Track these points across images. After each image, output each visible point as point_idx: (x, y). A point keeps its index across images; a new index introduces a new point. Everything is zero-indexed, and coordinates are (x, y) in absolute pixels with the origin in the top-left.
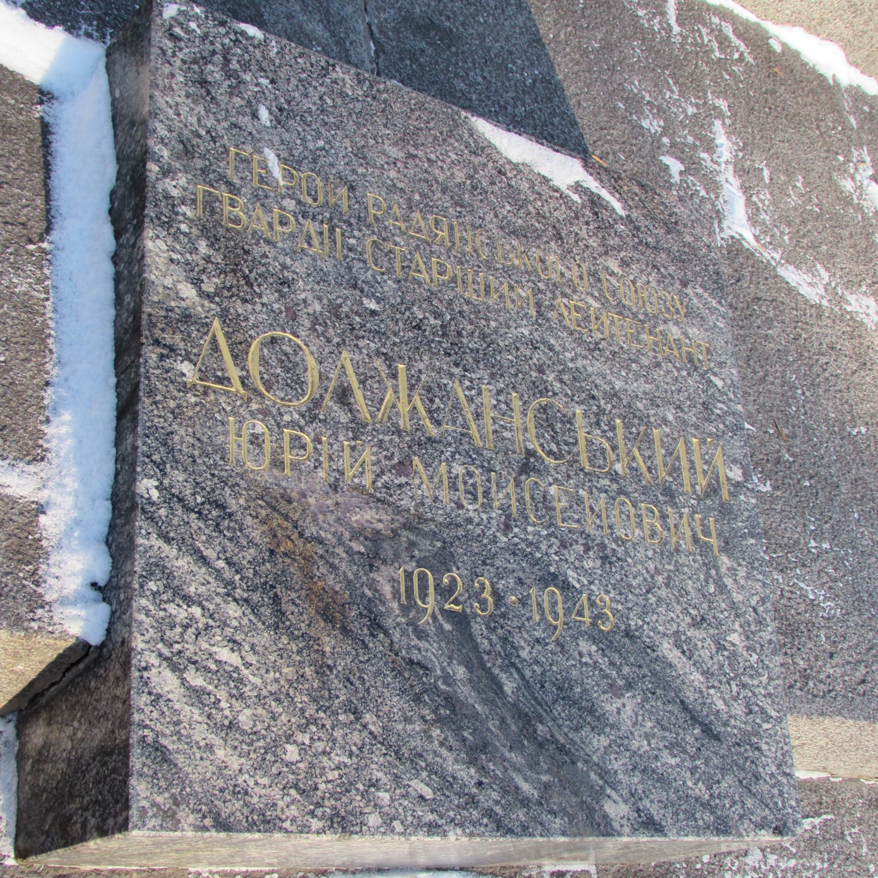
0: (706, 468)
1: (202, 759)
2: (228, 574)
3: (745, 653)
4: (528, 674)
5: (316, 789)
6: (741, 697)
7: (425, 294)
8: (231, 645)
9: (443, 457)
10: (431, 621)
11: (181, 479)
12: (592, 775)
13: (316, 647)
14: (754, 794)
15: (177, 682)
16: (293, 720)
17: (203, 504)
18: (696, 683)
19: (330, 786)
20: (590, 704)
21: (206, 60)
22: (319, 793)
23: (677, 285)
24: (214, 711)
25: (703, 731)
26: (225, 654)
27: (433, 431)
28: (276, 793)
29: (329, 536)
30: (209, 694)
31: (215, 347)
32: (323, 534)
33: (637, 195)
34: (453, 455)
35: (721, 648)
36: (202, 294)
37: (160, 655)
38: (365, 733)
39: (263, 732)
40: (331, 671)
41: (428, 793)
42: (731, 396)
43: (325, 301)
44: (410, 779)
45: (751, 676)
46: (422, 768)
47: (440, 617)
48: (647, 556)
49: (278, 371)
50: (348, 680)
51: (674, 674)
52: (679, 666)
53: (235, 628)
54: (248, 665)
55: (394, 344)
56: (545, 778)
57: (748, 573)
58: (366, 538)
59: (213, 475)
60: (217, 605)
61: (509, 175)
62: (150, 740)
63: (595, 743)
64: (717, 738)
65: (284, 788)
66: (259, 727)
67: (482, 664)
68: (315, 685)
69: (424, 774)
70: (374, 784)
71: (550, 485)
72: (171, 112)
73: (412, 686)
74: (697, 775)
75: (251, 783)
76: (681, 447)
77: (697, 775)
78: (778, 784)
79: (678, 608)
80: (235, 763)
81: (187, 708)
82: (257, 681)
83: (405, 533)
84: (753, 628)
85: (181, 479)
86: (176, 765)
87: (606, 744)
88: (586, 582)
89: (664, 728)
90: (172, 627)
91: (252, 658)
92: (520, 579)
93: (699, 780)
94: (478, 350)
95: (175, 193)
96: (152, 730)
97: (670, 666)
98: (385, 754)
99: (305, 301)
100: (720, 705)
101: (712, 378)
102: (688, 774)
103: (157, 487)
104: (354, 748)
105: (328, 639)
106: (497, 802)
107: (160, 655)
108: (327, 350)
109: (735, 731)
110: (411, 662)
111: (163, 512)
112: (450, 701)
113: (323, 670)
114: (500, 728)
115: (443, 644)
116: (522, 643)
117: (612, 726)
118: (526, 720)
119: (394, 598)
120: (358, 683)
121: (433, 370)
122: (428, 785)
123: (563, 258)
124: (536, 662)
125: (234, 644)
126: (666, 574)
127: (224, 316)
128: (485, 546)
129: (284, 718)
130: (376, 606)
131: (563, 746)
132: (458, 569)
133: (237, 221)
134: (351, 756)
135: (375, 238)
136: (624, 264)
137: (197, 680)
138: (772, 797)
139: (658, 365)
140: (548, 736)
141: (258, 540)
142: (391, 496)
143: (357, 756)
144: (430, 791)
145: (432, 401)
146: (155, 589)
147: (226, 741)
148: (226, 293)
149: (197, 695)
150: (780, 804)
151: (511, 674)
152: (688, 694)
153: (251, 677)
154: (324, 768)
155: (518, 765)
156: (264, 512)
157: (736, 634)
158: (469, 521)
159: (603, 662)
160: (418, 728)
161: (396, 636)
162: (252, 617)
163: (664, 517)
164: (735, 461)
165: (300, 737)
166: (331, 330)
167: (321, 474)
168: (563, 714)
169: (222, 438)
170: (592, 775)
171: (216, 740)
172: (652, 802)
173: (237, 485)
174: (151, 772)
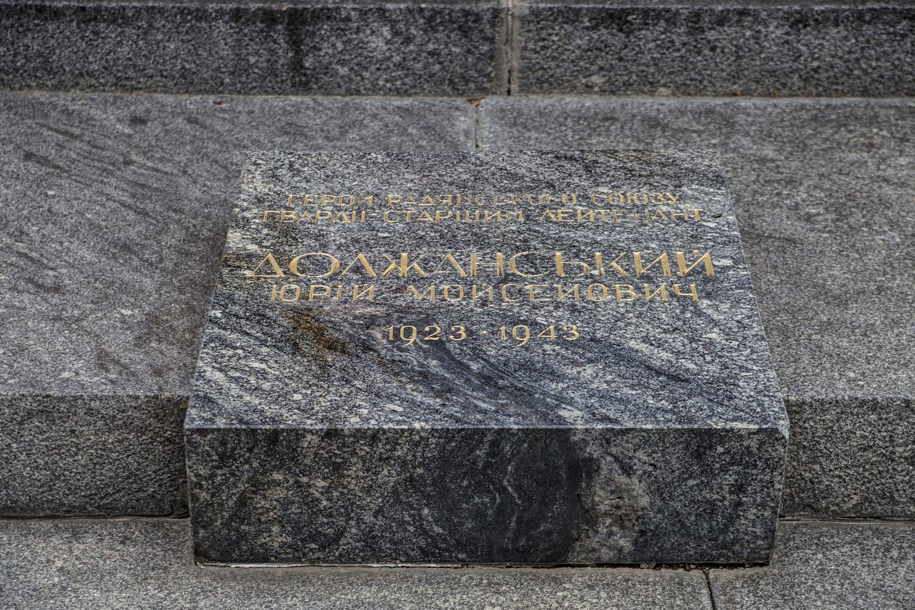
2: (263, 337)
3: (723, 342)
4: (493, 360)
5: (313, 409)
12: (548, 400)
21: (277, 168)
23: (672, 188)
26: (256, 365)
27: (426, 275)
36: (261, 247)
41: (400, 409)
47: (420, 343)
54: (270, 368)
64: (687, 381)
67: (453, 359)
70: (359, 407)
79: (649, 327)
80: (257, 401)
84: (736, 330)
97: (637, 351)
100: (692, 366)
101: (704, 223)
106: (457, 412)
110: (394, 361)
113: (324, 367)
114: (465, 383)
115: (421, 353)
124: (502, 355)
125: (262, 361)
127: (275, 252)
134: (341, 396)
149: (236, 380)
158: (452, 305)
159: (568, 354)
164: (726, 257)
165: (304, 391)
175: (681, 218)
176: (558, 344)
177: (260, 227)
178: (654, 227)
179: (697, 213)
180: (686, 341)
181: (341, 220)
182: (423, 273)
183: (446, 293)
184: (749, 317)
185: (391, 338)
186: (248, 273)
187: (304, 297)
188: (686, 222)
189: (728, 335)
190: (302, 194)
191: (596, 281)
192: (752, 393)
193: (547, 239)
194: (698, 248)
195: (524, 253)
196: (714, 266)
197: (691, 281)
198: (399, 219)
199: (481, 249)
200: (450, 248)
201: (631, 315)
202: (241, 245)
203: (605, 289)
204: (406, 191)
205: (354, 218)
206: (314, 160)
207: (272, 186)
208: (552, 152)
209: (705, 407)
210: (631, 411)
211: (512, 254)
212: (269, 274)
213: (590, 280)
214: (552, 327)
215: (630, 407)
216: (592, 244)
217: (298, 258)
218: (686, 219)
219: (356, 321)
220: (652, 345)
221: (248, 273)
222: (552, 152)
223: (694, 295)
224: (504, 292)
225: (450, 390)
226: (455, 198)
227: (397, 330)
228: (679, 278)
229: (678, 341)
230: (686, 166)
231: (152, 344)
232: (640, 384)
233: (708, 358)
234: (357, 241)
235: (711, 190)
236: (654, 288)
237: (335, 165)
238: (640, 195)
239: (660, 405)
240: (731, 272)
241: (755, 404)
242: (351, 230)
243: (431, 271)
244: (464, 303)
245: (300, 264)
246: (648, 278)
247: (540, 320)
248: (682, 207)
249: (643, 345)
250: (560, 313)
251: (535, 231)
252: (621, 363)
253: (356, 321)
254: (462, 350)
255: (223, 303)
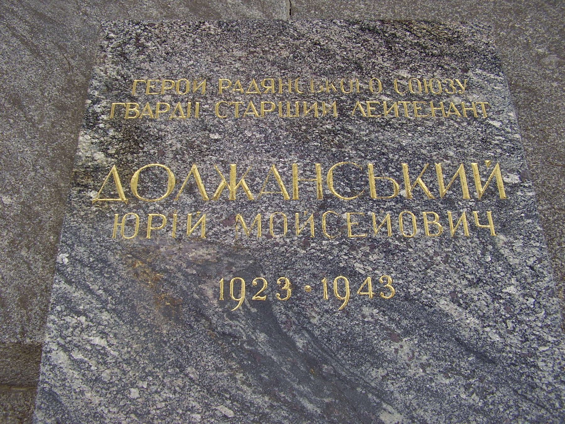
0: (484, 180)
1: (76, 398)
3: (521, 299)
4: (317, 333)
5: (149, 413)
6: (517, 330)
7: (254, 122)
8: (101, 335)
9: (259, 210)
10: (241, 308)
11: (82, 251)
12: (370, 396)
13: (157, 331)
14: (530, 400)
15: (66, 357)
16: (137, 374)
17: (93, 261)
18: (472, 325)
19: (158, 411)
20: (371, 348)
21: (125, 44)
22: (150, 416)
23: (459, 72)
24: (86, 372)
25: (477, 358)
26: (97, 340)
27: (252, 196)
28: (122, 416)
29: (172, 268)
30: (85, 363)
31: (112, 179)
32: (168, 267)
33: (424, 29)
34: (266, 208)
35: (496, 298)
36: (108, 155)
37: (58, 344)
38: (187, 379)
39: (117, 382)
40: (166, 344)
41: (230, 414)
42: (509, 130)
43: (184, 142)
44: (217, 406)
45: (528, 315)
46: (226, 398)
48: (426, 245)
49: (149, 184)
50: (177, 348)
51: (450, 320)
52: (455, 315)
53: (106, 326)
54: (110, 345)
55: (229, 154)
56: (326, 400)
57: (524, 243)
58: (198, 265)
59: (101, 246)
60: (95, 314)
61: (322, 44)
62: (47, 389)
63: (374, 374)
64: (493, 361)
65: (127, 413)
66: (114, 379)
67: (279, 331)
68: (154, 353)
69: (228, 402)
70: (192, 410)
71: (343, 213)
72: (102, 73)
73: (223, 349)
74: (471, 390)
75: (106, 411)
76: (461, 170)
77: (471, 390)
78: (555, 390)
79: (455, 276)
80: (97, 400)
81: (71, 371)
82: (116, 354)
83: (226, 259)
84: (530, 280)
85: (82, 251)
86: (61, 403)
87: (383, 374)
88: (370, 269)
89: (438, 359)
90: (67, 328)
91: (114, 341)
92: (314, 274)
93: (472, 393)
94: (291, 145)
95: (99, 110)
96: (49, 384)
97: (447, 315)
98: (199, 391)
99: (171, 145)
100: (496, 338)
101: (491, 122)
102: (463, 389)
103: (67, 257)
104: (177, 388)
105: (165, 326)
106: (285, 418)
107: (58, 344)
108: (182, 167)
109: (511, 355)
110: (224, 334)
111: (69, 269)
112: (254, 355)
113: (160, 344)
114: (291, 370)
116: (313, 314)
117: (390, 362)
118: (312, 363)
119: (215, 297)
120: (184, 350)
121: (256, 163)
122: (230, 408)
123: (361, 79)
124: (325, 325)
125: (103, 334)
126: (444, 255)
128: (288, 257)
129: (131, 373)
130: (201, 303)
131: (345, 377)
132: (265, 274)
133: (134, 114)
134: (175, 392)
135: (222, 101)
136: (413, 70)
137: (77, 355)
138: (550, 399)
139: (442, 124)
140: (332, 372)
141: (125, 276)
142: (218, 239)
143: (179, 393)
144: (232, 412)
145: (253, 180)
146: (60, 310)
147: (92, 388)
148: (122, 151)
149: (77, 364)
150: (557, 405)
151: (303, 335)
152: (464, 333)
153: (112, 352)
154: (155, 401)
155: (305, 393)
156: (130, 261)
157: (512, 287)
158: (277, 244)
160: (225, 374)
161: (214, 320)
162: (117, 319)
163: (443, 218)
164: (512, 171)
165: (140, 384)
166: (187, 156)
167: (171, 234)
168: (346, 357)
169: (109, 225)
170: (370, 396)
171: (85, 387)
172: (425, 411)
173: (116, 248)
174: (46, 406)
175: (470, 114)
176: (375, 305)
177: (108, 126)
178: (449, 126)
179: (483, 106)
180: (490, 299)
181: (178, 115)
182: (252, 196)
183: (271, 226)
184: (540, 261)
185: (222, 298)
186: (94, 195)
187: (142, 233)
188: (475, 119)
189: (524, 288)
190: (146, 77)
191: (405, 207)
192: (551, 379)
193: (359, 143)
194: (488, 158)
195: (341, 164)
196: (505, 183)
197: (487, 206)
198: (228, 112)
199: (301, 157)
200: (274, 156)
201: (439, 258)
202: (88, 154)
203: (414, 218)
204: (234, 74)
205: (189, 110)
206: (157, 31)
207: (120, 67)
208: (357, 23)
209: (511, 403)
210: (445, 412)
211: (329, 167)
212: (112, 196)
213: (399, 205)
214: (369, 279)
215: (446, 406)
216: (398, 150)
217: (138, 171)
218: (476, 115)
219: (188, 270)
220: (460, 305)
221: (94, 195)
222: (357, 23)
223: (491, 226)
224: (324, 223)
225: (277, 382)
226: (277, 83)
227: (227, 283)
228: (477, 200)
229: (480, 296)
230: (469, 43)
231: (23, 253)
232: (452, 369)
233: (510, 325)
234: (190, 145)
235: (492, 76)
236: (456, 215)
237: (174, 38)
238: (434, 82)
239: (472, 402)
240: (519, 193)
241: (552, 396)
242: (185, 129)
243: (257, 192)
244: (288, 240)
245: (141, 181)
246: (449, 202)
247: (359, 267)
248: (470, 98)
249: (452, 305)
250: (375, 257)
251: (349, 132)
252: (434, 335)
253: (188, 270)
254: (287, 316)
255: (69, 242)
